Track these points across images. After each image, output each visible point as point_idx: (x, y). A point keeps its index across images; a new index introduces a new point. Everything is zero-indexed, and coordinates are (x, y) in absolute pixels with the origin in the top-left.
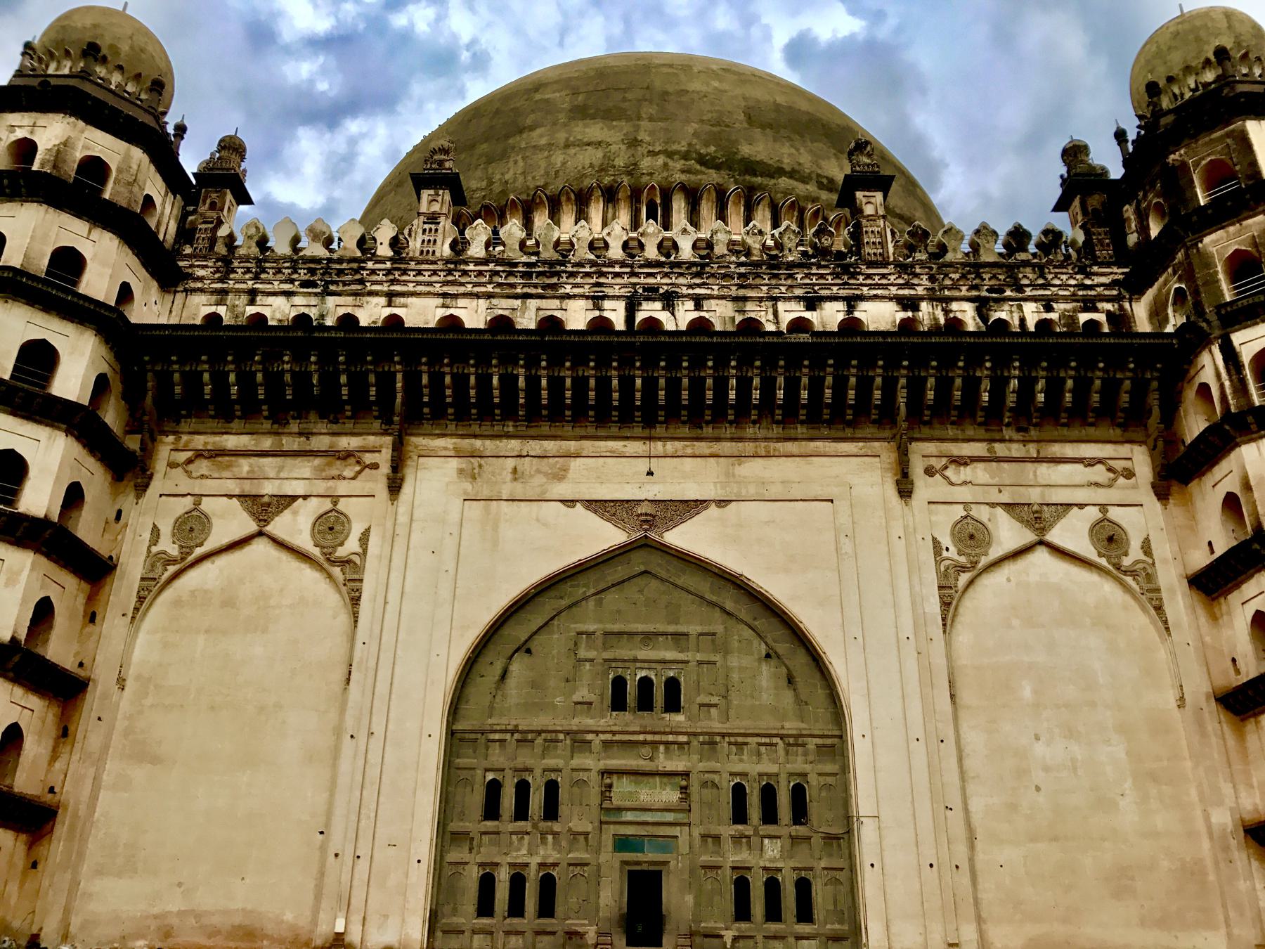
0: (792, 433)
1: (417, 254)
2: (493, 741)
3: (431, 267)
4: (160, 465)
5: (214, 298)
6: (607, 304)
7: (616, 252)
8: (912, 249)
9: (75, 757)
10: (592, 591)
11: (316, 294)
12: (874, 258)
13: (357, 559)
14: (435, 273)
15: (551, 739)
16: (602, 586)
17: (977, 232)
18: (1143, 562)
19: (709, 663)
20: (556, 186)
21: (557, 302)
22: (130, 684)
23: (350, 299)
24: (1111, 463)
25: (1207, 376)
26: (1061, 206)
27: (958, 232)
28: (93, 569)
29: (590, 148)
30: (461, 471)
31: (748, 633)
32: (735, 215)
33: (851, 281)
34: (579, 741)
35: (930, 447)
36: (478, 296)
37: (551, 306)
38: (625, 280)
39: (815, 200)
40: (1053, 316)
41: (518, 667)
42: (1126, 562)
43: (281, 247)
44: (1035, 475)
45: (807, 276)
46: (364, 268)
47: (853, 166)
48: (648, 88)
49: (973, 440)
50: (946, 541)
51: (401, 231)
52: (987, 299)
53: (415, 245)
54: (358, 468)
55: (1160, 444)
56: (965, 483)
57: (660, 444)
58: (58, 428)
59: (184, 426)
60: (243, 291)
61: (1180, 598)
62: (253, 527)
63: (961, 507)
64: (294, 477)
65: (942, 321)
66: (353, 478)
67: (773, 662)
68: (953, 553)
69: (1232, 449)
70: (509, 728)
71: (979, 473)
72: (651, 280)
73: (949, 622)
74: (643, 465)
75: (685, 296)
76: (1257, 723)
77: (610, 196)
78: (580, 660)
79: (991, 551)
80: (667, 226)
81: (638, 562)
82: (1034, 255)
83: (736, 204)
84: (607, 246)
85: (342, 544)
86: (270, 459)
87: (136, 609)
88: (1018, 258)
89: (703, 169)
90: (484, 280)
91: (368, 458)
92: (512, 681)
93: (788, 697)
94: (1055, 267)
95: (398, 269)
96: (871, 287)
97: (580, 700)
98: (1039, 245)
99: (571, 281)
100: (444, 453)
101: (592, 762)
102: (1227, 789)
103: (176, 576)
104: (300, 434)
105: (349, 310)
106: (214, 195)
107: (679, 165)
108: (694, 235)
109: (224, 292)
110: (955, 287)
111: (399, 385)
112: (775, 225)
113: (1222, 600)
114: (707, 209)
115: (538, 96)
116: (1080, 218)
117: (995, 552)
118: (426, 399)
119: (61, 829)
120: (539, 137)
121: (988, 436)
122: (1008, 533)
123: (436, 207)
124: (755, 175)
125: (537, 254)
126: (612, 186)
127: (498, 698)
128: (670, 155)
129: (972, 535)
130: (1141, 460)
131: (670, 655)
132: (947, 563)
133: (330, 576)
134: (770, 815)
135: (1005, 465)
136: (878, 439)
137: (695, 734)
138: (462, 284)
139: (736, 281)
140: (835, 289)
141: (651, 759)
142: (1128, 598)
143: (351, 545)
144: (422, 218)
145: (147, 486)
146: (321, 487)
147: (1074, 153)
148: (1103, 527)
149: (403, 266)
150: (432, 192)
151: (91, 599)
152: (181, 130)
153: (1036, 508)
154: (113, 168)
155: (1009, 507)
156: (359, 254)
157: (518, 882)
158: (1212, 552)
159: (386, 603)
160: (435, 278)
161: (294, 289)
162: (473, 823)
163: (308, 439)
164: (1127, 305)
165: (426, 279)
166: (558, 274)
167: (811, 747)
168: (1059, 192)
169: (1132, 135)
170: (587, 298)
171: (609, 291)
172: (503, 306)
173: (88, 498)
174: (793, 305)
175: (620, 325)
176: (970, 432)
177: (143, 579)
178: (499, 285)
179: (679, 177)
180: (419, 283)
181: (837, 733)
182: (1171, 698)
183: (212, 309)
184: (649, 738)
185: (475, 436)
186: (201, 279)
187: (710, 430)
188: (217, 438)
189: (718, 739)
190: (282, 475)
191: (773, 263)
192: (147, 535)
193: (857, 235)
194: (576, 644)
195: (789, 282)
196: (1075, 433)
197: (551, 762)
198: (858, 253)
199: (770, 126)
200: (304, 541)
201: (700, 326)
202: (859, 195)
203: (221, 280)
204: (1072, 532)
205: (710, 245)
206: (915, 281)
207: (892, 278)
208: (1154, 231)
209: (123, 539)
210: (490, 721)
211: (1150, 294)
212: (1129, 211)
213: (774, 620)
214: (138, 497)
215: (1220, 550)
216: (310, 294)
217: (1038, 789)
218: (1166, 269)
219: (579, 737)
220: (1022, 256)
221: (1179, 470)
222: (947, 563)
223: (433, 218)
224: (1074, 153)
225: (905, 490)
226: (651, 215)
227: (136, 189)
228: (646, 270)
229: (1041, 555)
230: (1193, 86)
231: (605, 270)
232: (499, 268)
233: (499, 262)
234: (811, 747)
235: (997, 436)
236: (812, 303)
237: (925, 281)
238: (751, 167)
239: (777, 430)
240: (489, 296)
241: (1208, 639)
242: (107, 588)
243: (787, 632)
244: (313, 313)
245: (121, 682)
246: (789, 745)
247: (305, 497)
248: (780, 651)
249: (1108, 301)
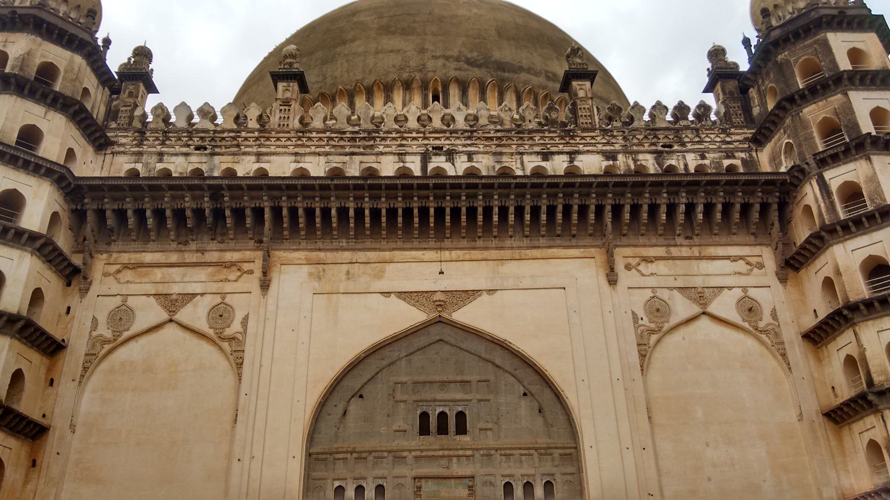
0: (536, 243)
1: (276, 126)
2: (339, 459)
3: (287, 135)
5: (133, 158)
6: (408, 158)
8: (610, 119)
9: (42, 481)
10: (404, 354)
11: (206, 155)
12: (586, 126)
13: (240, 336)
14: (289, 139)
15: (378, 456)
16: (411, 350)
17: (654, 107)
18: (772, 324)
19: (485, 400)
21: (373, 158)
22: (79, 430)
23: (230, 158)
24: (749, 259)
25: (809, 200)
26: (707, 90)
27: (642, 107)
28: (51, 347)
29: (391, 55)
30: (310, 274)
31: (511, 379)
32: (492, 96)
33: (571, 141)
34: (398, 457)
35: (628, 251)
36: (319, 154)
37: (370, 161)
38: (420, 142)
39: (544, 88)
40: (707, 162)
41: (355, 407)
44: (698, 268)
45: (542, 138)
46: (239, 137)
47: (570, 65)
48: (430, 13)
49: (656, 246)
50: (641, 313)
51: (264, 111)
53: (275, 120)
54: (239, 273)
55: (780, 246)
56: (652, 274)
57: (447, 253)
58: (26, 250)
59: (114, 247)
60: (154, 153)
61: (797, 348)
62: (165, 316)
63: (650, 290)
64: (194, 280)
65: (633, 167)
66: (236, 281)
67: (529, 398)
68: (646, 321)
69: (827, 248)
70: (350, 449)
71: (661, 267)
72: (437, 142)
73: (645, 368)
74: (436, 267)
75: (460, 152)
76: (850, 429)
77: (407, 86)
78: (397, 402)
79: (671, 320)
80: (446, 106)
81: (435, 332)
82: (692, 122)
83: (493, 91)
84: (406, 119)
85: (229, 326)
86: (176, 269)
87: (82, 376)
88: (681, 123)
89: (469, 67)
90: (323, 143)
91: (246, 267)
92: (350, 417)
93: (540, 421)
94: (706, 130)
95: (264, 137)
96: (585, 145)
97: (397, 428)
98: (696, 115)
99: (383, 143)
100: (301, 262)
101: (407, 471)
102: (833, 474)
103: (110, 352)
104: (197, 251)
105: (230, 165)
106: (131, 87)
107: (453, 65)
108: (465, 112)
109: (140, 154)
110: (641, 144)
111: (267, 215)
112: (519, 103)
113: (824, 348)
114: (473, 94)
115: (355, 19)
116: (721, 97)
117: (674, 320)
118: (285, 225)
120: (358, 46)
121: (666, 243)
122: (682, 308)
123: (288, 95)
124: (504, 71)
125: (359, 125)
126: (408, 80)
127: (341, 430)
128: (447, 58)
129: (658, 309)
130: (768, 257)
131: (459, 396)
132: (642, 328)
133: (221, 349)
135: (678, 262)
136: (593, 246)
137: (477, 449)
138: (308, 146)
139: (495, 142)
140: (561, 146)
141: (448, 468)
142: (763, 349)
143: (235, 327)
144: (279, 102)
145: (88, 289)
146: (214, 287)
147: (717, 54)
148: (745, 302)
149: (266, 135)
150: (285, 84)
151: (50, 369)
152: (107, 42)
153: (700, 290)
154: (62, 70)
156: (235, 127)
158: (817, 317)
159: (261, 366)
160: (289, 143)
161: (190, 151)
163: (203, 254)
164: (754, 154)
165: (283, 143)
166: (374, 138)
167: (556, 455)
168: (707, 80)
169: (754, 42)
170: (394, 154)
171: (409, 150)
172: (337, 161)
173: (47, 297)
174: (533, 158)
175: (417, 172)
176: (654, 241)
177: (87, 355)
178: (334, 146)
179: (453, 74)
180: (278, 146)
181: (574, 445)
182: (793, 415)
183: (132, 166)
184: (446, 453)
185: (320, 250)
186: (123, 145)
187: (481, 242)
188: (138, 255)
189: (493, 452)
190: (185, 280)
191: (519, 130)
192: (89, 324)
193: (574, 111)
194: (394, 391)
195: (530, 142)
196: (724, 240)
197: (378, 472)
198: (576, 123)
199: (514, 39)
200: (202, 324)
201: (472, 173)
202: (575, 84)
203: (137, 146)
204: (725, 305)
205: (476, 118)
206: (614, 141)
207: (599, 138)
208: (771, 106)
209: (72, 327)
210: (335, 446)
211: (768, 148)
212: (753, 93)
213: (529, 370)
214: (82, 297)
215: (822, 315)
216: (201, 155)
217: (709, 479)
218: (779, 130)
219: (398, 454)
220: (683, 123)
221: (793, 263)
222: (642, 328)
223: (286, 103)
224: (717, 54)
225: (612, 280)
226: (436, 98)
227: (78, 84)
228: (434, 135)
229: (704, 321)
230: (791, 10)
231: (406, 135)
232: (333, 135)
233: (332, 131)
234: (556, 455)
235: (672, 243)
236: (546, 156)
237: (620, 140)
238: (501, 66)
239: (526, 242)
240: (327, 154)
241: (816, 375)
242: (61, 362)
243: (537, 377)
244: (204, 168)
245: (73, 428)
246: (541, 454)
247: (202, 294)
248: (533, 391)
249: (742, 152)
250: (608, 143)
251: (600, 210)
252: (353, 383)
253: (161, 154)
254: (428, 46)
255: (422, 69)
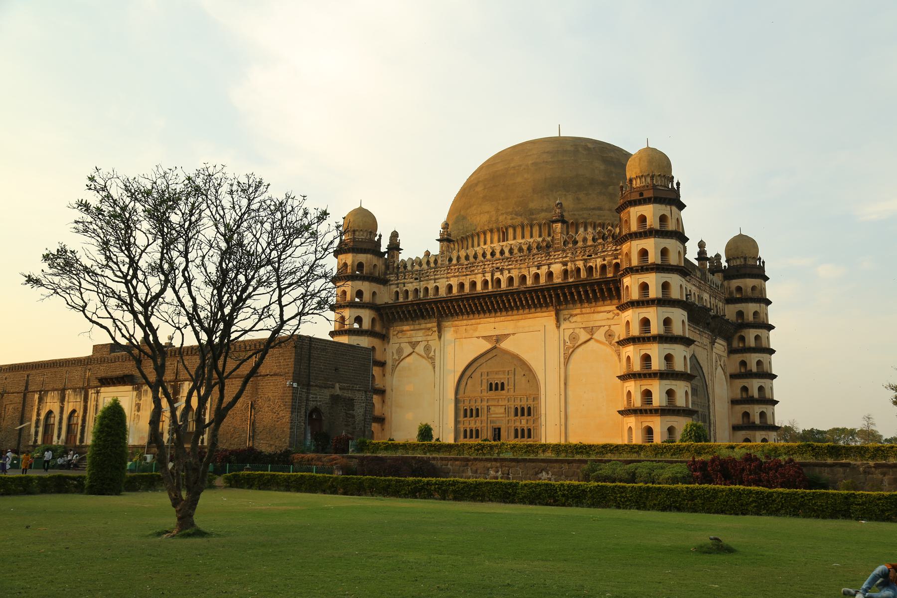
4: (391, 336)
7: (489, 256)
20: (478, 229)
35: (566, 312)
37: (472, 278)
40: (605, 262)
42: (613, 342)
43: (409, 268)
50: (567, 340)
52: (585, 260)
62: (411, 350)
64: (419, 336)
71: (577, 318)
74: (492, 325)
77: (491, 231)
81: (494, 352)
101: (485, 404)
107: (509, 217)
117: (580, 342)
119: (386, 422)
122: (584, 336)
128: (507, 213)
129: (574, 337)
134: (523, 415)
143: (432, 353)
146: (424, 338)
151: (383, 371)
152: (380, 236)
155: (584, 328)
157: (471, 431)
162: (461, 418)
172: (462, 279)
179: (509, 222)
225: (558, 327)
229: (592, 342)
237: (569, 255)
240: (458, 276)
250: (566, 257)
251: (550, 296)
252: (468, 373)
253: (404, 283)
254: (500, 207)
255: (497, 221)
